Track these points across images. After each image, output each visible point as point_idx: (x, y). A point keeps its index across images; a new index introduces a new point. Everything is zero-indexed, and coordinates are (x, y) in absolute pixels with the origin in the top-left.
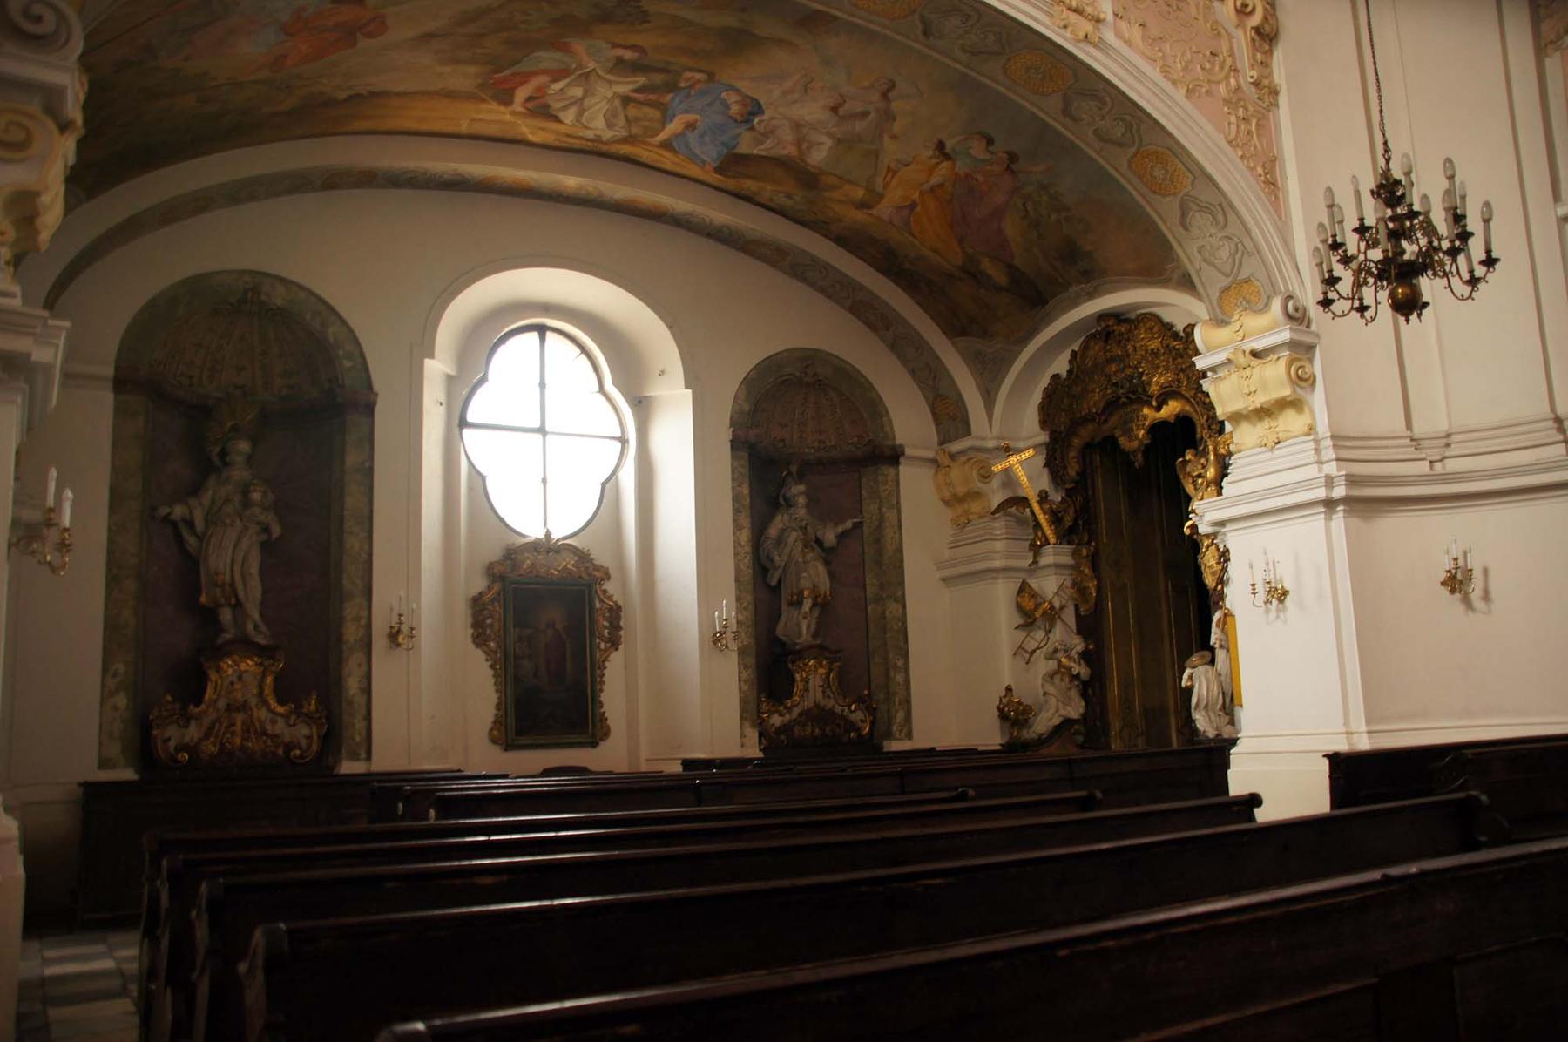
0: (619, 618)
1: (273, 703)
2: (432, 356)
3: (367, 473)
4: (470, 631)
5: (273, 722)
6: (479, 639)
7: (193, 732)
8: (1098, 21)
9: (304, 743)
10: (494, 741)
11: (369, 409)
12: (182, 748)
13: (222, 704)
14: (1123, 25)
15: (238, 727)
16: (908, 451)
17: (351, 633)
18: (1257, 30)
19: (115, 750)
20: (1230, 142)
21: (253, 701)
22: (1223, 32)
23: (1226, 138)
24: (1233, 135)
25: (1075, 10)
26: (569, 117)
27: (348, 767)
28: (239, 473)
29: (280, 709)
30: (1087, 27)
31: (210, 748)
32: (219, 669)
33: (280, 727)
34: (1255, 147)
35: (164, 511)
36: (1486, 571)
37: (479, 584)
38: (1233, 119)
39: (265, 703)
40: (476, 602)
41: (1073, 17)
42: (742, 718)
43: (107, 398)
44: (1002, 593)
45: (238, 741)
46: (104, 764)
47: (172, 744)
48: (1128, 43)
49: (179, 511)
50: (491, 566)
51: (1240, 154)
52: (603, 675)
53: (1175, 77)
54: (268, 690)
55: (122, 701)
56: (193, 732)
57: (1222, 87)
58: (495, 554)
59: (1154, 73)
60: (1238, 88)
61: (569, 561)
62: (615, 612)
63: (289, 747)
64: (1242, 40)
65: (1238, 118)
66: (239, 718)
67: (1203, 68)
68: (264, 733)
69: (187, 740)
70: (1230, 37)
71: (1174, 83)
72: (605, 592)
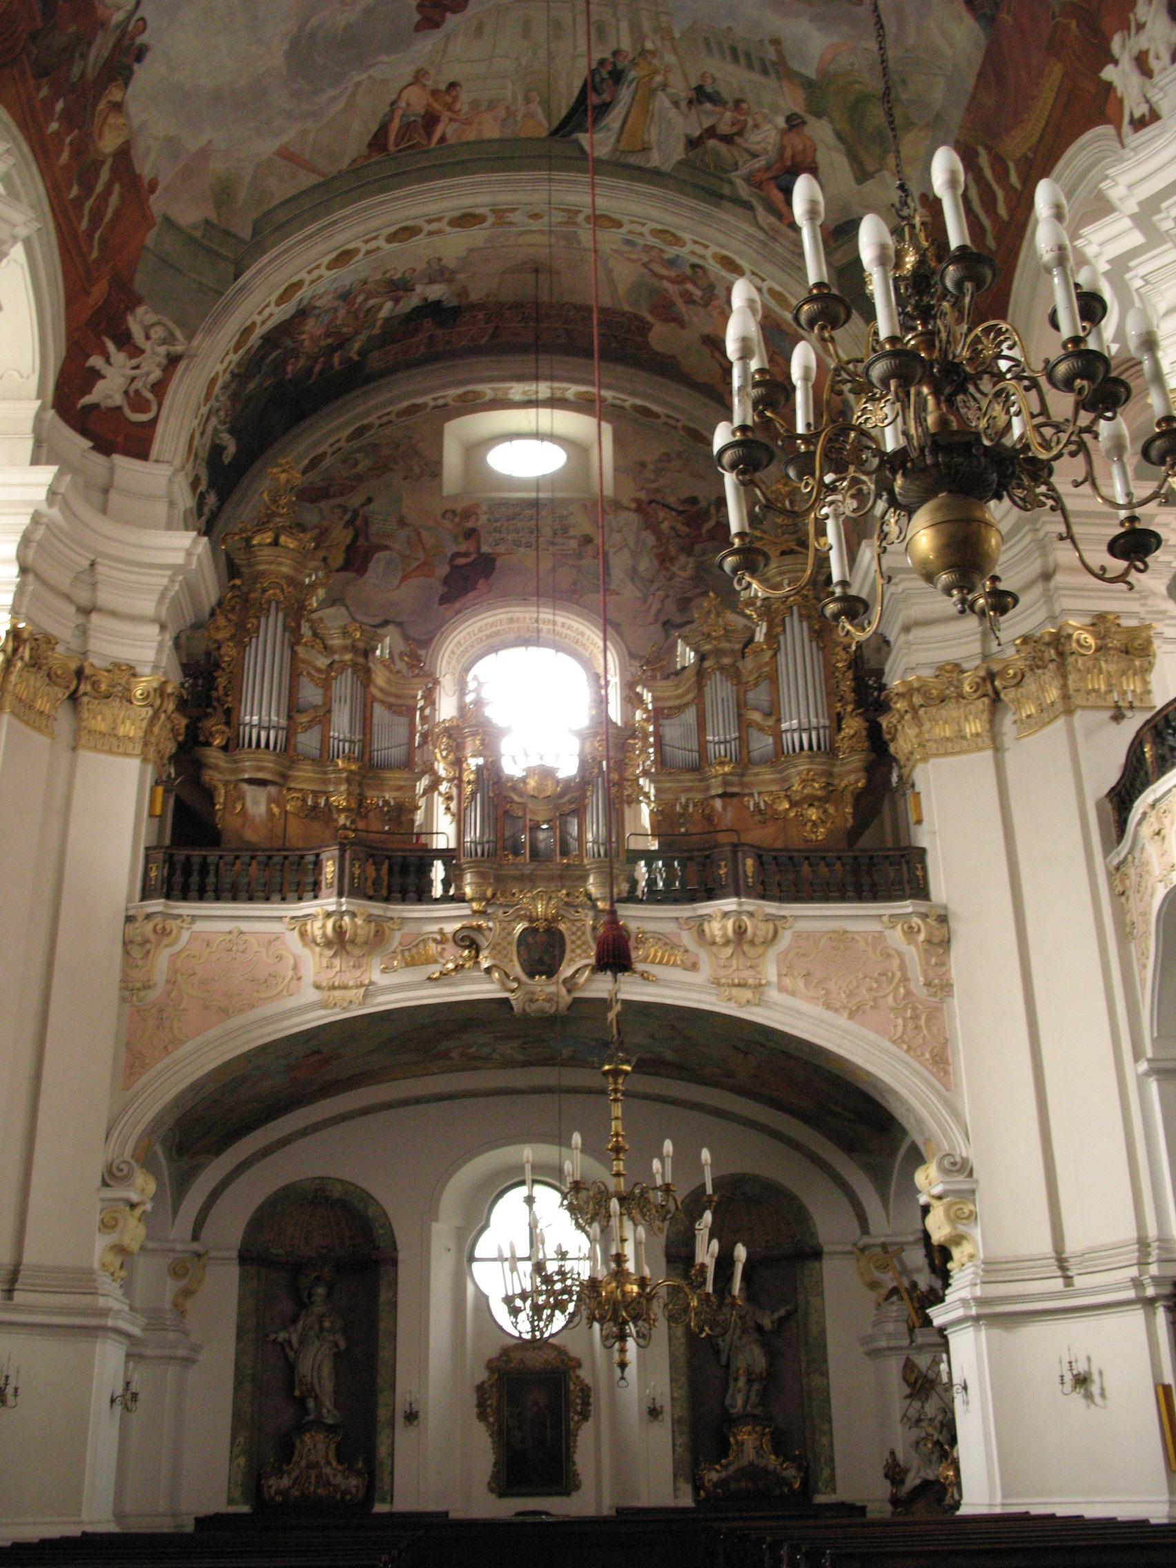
0: (589, 1397)
1: (334, 1463)
2: (437, 1220)
3: (394, 1305)
4: (475, 1410)
5: (335, 1476)
6: (482, 1416)
7: (285, 1482)
8: (761, 985)
9: (354, 1490)
10: (491, 1490)
11: (395, 1262)
12: (278, 1492)
13: (303, 1463)
14: (787, 981)
15: (313, 1479)
16: (826, 1249)
17: (382, 1414)
18: (928, 941)
19: (237, 1494)
20: (894, 1042)
21: (323, 1462)
22: (893, 952)
23: (890, 1039)
24: (899, 1033)
25: (739, 985)
26: (495, 1056)
27: (379, 1508)
28: (318, 1309)
29: (340, 1468)
30: (747, 994)
31: (295, 1493)
32: (302, 1441)
33: (339, 1479)
34: (924, 1037)
35: (272, 1337)
36: (1101, 1373)
37: (482, 1375)
38: (900, 1021)
39: (329, 1463)
40: (480, 1389)
41: (735, 991)
42: (675, 1476)
43: (234, 1270)
44: (894, 1365)
45: (312, 1488)
46: (231, 1501)
47: (273, 1490)
48: (793, 994)
49: (282, 1336)
50: (490, 1361)
51: (905, 1047)
52: (575, 1441)
53: (838, 1005)
54: (331, 1454)
55: (242, 1461)
56: (285, 1482)
57: (890, 999)
58: (493, 1352)
59: (818, 1011)
60: (908, 993)
61: (550, 1355)
62: (586, 1392)
63: (344, 1493)
64: (912, 953)
65: (904, 1019)
66: (313, 1473)
67: (870, 989)
68: (329, 1483)
69: (282, 1487)
70: (900, 955)
71: (836, 1010)
72: (578, 1377)
